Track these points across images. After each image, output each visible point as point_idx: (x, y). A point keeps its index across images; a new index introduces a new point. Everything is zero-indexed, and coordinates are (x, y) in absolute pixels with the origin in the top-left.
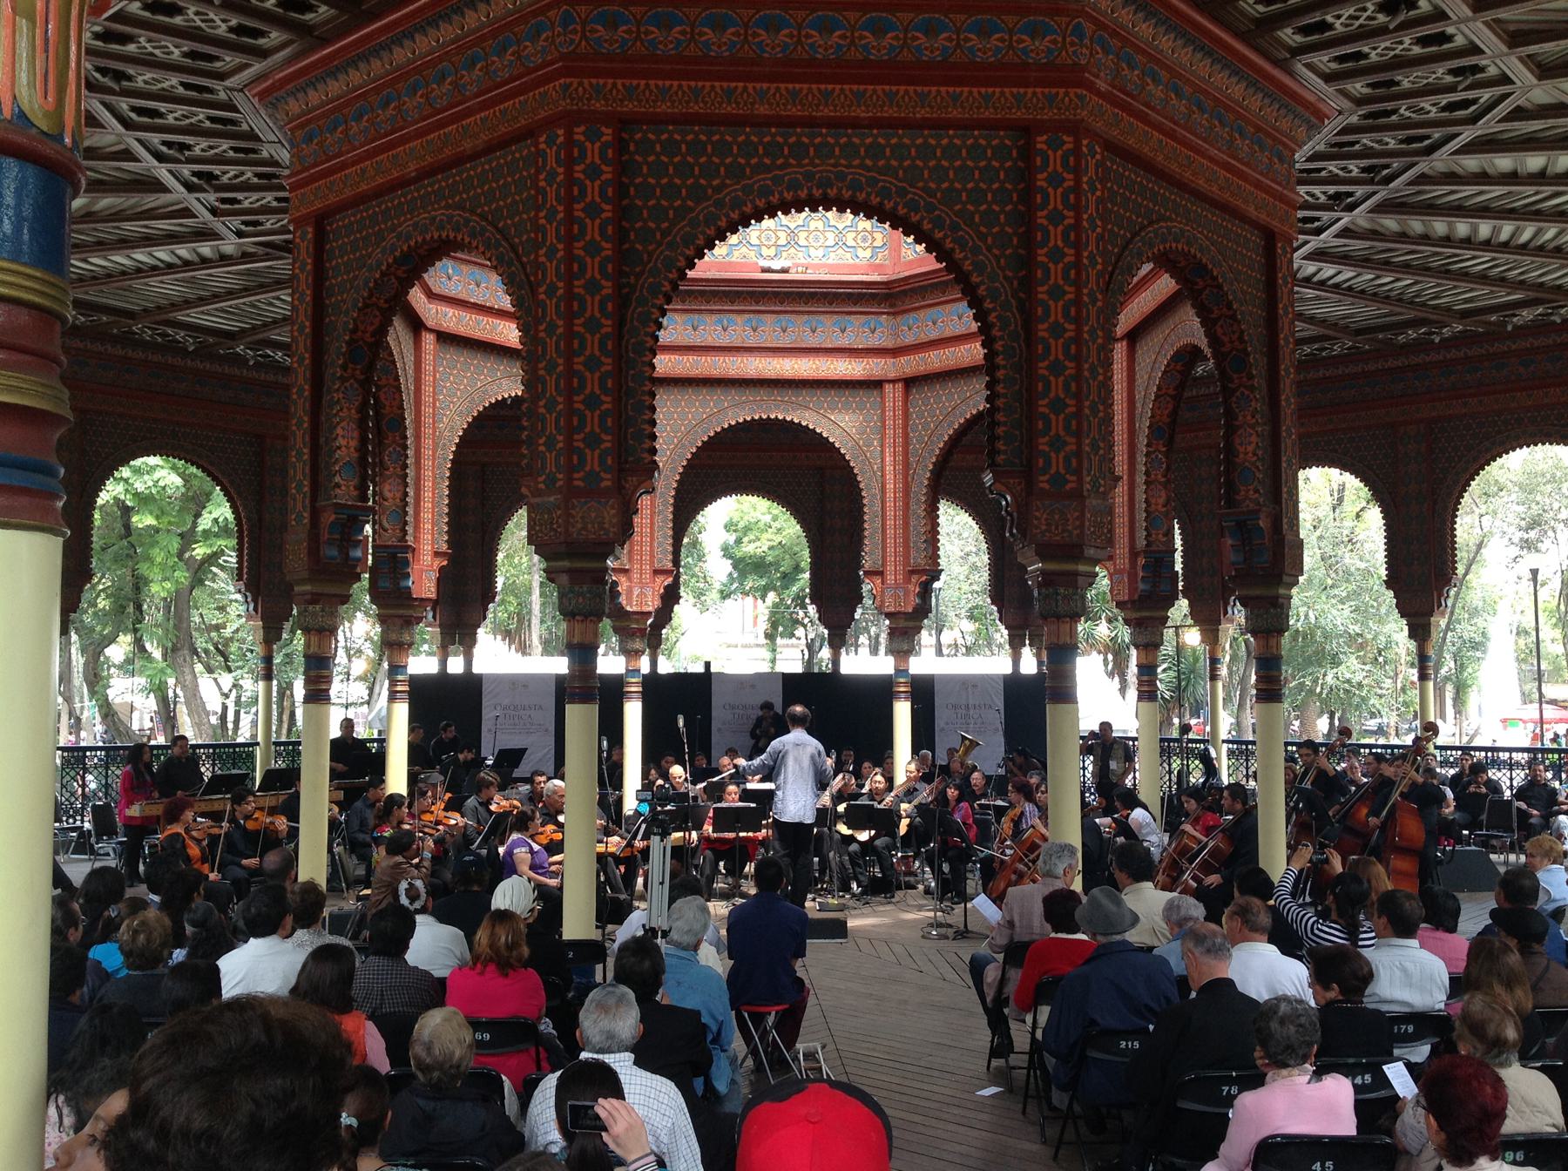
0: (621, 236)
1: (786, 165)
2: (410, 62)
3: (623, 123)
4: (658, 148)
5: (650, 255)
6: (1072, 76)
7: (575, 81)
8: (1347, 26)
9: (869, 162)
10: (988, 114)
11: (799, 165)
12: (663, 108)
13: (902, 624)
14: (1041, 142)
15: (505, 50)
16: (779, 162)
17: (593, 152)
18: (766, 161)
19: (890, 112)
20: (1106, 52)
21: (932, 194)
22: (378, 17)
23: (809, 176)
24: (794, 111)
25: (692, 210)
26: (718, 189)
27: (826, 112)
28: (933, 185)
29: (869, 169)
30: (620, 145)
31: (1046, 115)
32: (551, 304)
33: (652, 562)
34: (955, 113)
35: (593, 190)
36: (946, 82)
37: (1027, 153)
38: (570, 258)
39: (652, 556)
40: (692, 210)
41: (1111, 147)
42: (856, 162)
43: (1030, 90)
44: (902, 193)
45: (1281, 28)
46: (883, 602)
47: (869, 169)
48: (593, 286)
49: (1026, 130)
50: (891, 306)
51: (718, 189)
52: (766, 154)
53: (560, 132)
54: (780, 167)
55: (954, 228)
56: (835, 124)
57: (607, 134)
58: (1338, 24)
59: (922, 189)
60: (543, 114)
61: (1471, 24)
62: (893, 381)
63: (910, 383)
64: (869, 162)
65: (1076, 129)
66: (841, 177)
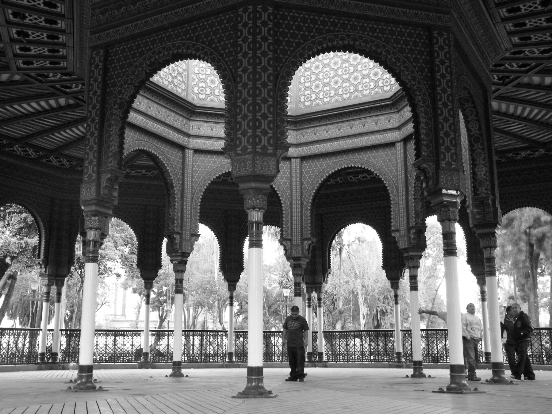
5: (286, 59)
16: (337, 29)
18: (332, 28)
26: (313, 37)
28: (395, 45)
29: (371, 36)
33: (190, 231)
39: (191, 228)
42: (366, 33)
47: (371, 36)
51: (313, 37)
54: (337, 31)
55: (404, 62)
56: (359, 17)
59: (391, 46)
64: (371, 34)
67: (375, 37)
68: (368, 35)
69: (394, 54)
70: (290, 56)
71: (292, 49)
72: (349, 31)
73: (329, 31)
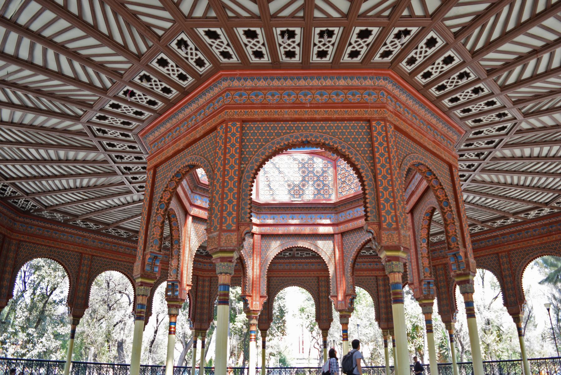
0: (241, 153)
1: (294, 132)
2: (183, 117)
3: (244, 121)
4: (254, 128)
5: (251, 158)
6: (383, 106)
7: (229, 111)
8: (464, 99)
9: (320, 131)
10: (357, 116)
11: (298, 132)
12: (256, 117)
13: (344, 313)
14: (374, 123)
15: (210, 107)
17: (234, 130)
19: (326, 116)
20: (391, 101)
21: (340, 139)
22: (175, 105)
23: (301, 135)
24: (297, 116)
25: (263, 145)
27: (306, 116)
28: (341, 137)
29: (320, 133)
30: (242, 128)
31: (376, 116)
32: (218, 174)
34: (346, 116)
35: (233, 140)
36: (343, 107)
37: (370, 127)
38: (225, 159)
40: (263, 145)
41: (397, 128)
43: (369, 110)
44: (331, 139)
45: (443, 100)
46: (337, 306)
47: (320, 133)
48: (232, 167)
49: (369, 121)
50: (336, 211)
52: (288, 129)
53: (224, 125)
57: (238, 124)
58: (461, 98)
60: (219, 121)
61: (501, 96)
62: (337, 234)
63: (343, 234)
64: (320, 131)
65: (384, 119)
66: (311, 135)
67: (324, 133)
68: (318, 132)
69: (340, 143)
70: (254, 155)
71: (255, 150)
72: (302, 131)
73: (286, 133)
